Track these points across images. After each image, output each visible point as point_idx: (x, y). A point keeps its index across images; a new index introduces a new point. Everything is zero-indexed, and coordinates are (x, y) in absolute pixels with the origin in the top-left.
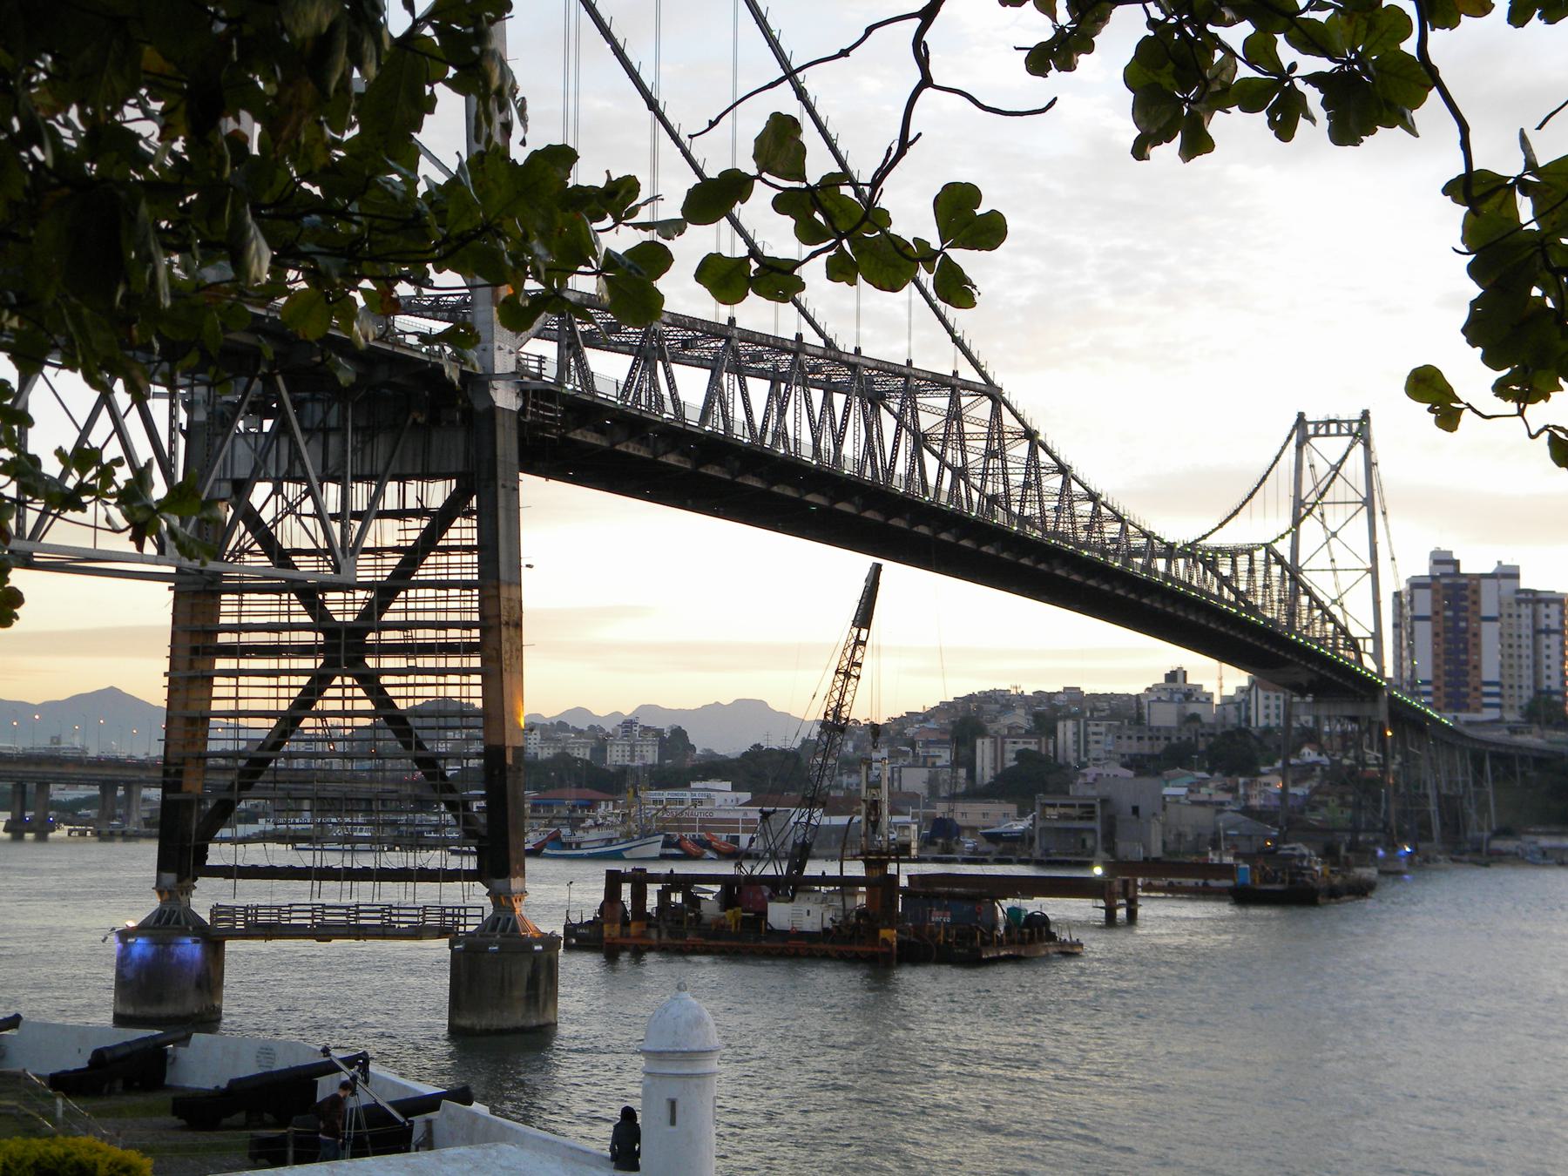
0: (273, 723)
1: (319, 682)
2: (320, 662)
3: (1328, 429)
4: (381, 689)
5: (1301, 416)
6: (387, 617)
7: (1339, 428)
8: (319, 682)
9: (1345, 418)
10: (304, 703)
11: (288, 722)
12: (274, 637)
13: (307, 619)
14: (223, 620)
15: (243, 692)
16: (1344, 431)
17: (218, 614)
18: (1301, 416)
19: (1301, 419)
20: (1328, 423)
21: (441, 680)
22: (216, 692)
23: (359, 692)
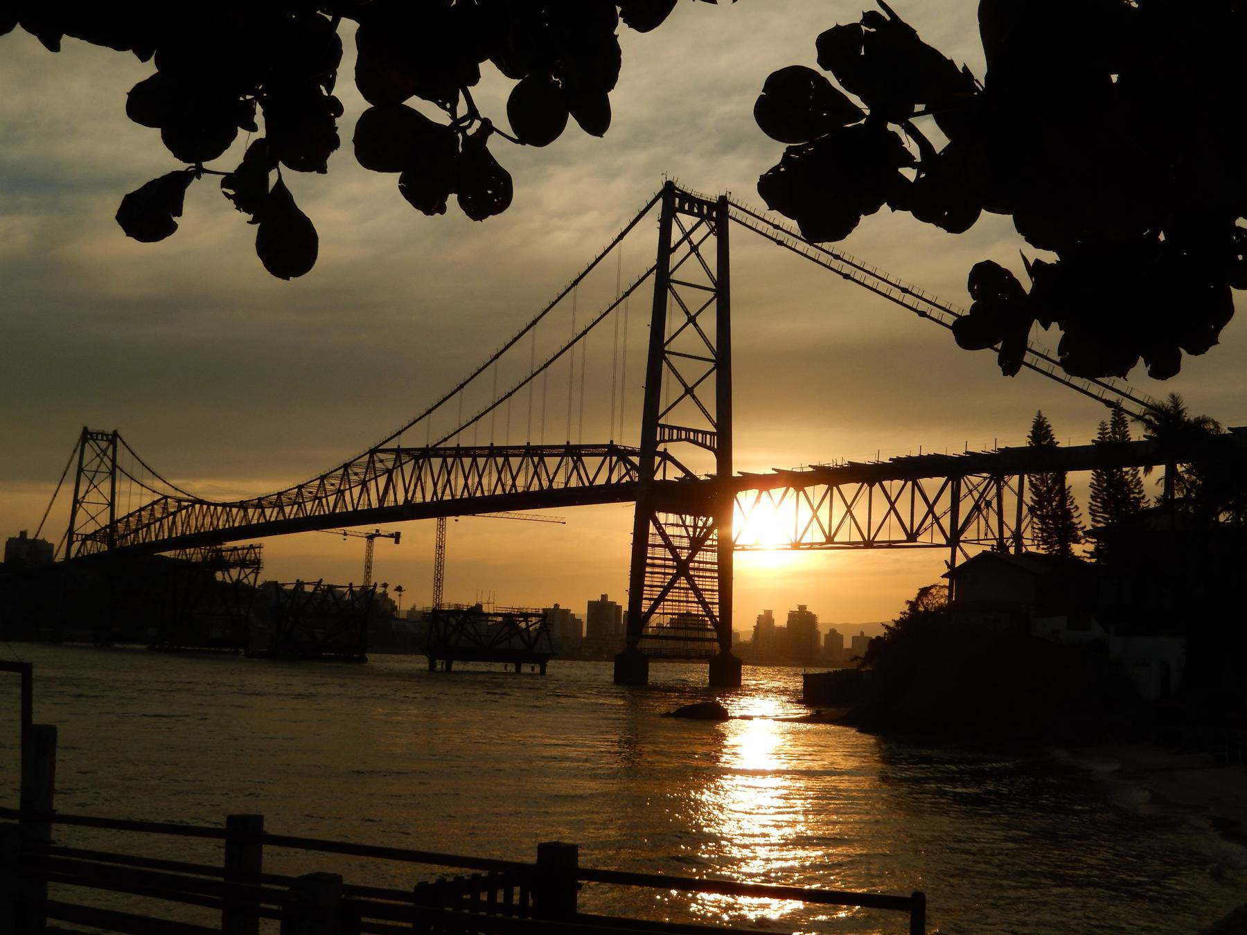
0: (662, 589)
1: (675, 578)
2: (675, 572)
3: (97, 436)
4: (694, 581)
5: (85, 429)
6: (696, 559)
7: (102, 437)
8: (675, 578)
9: (106, 433)
10: (671, 586)
11: (667, 589)
12: (663, 562)
13: (672, 557)
14: (648, 555)
15: (655, 580)
16: (105, 438)
17: (647, 554)
18: (85, 429)
19: (85, 430)
20: (97, 434)
21: (704, 579)
22: (646, 579)
23: (697, 582)
